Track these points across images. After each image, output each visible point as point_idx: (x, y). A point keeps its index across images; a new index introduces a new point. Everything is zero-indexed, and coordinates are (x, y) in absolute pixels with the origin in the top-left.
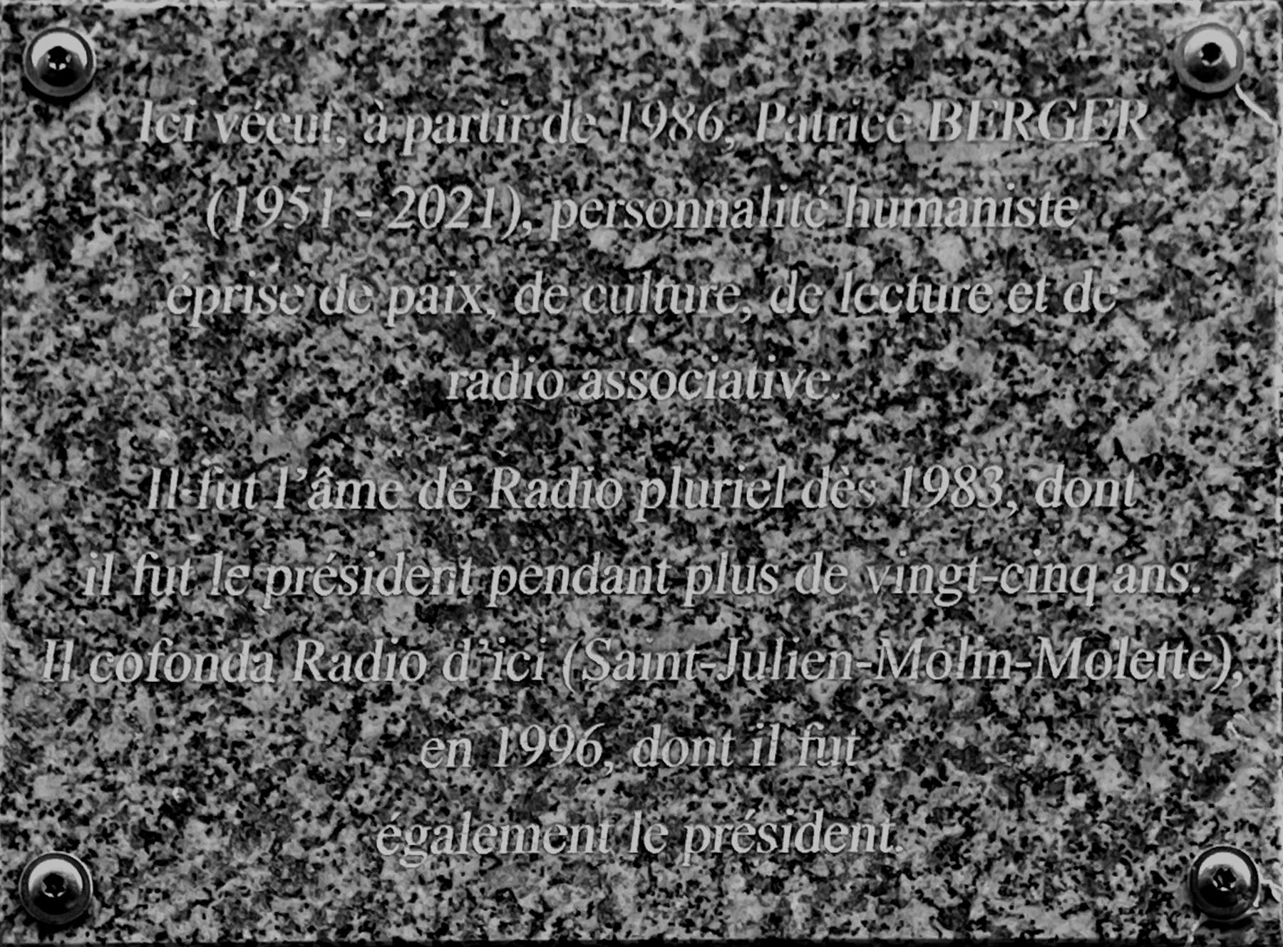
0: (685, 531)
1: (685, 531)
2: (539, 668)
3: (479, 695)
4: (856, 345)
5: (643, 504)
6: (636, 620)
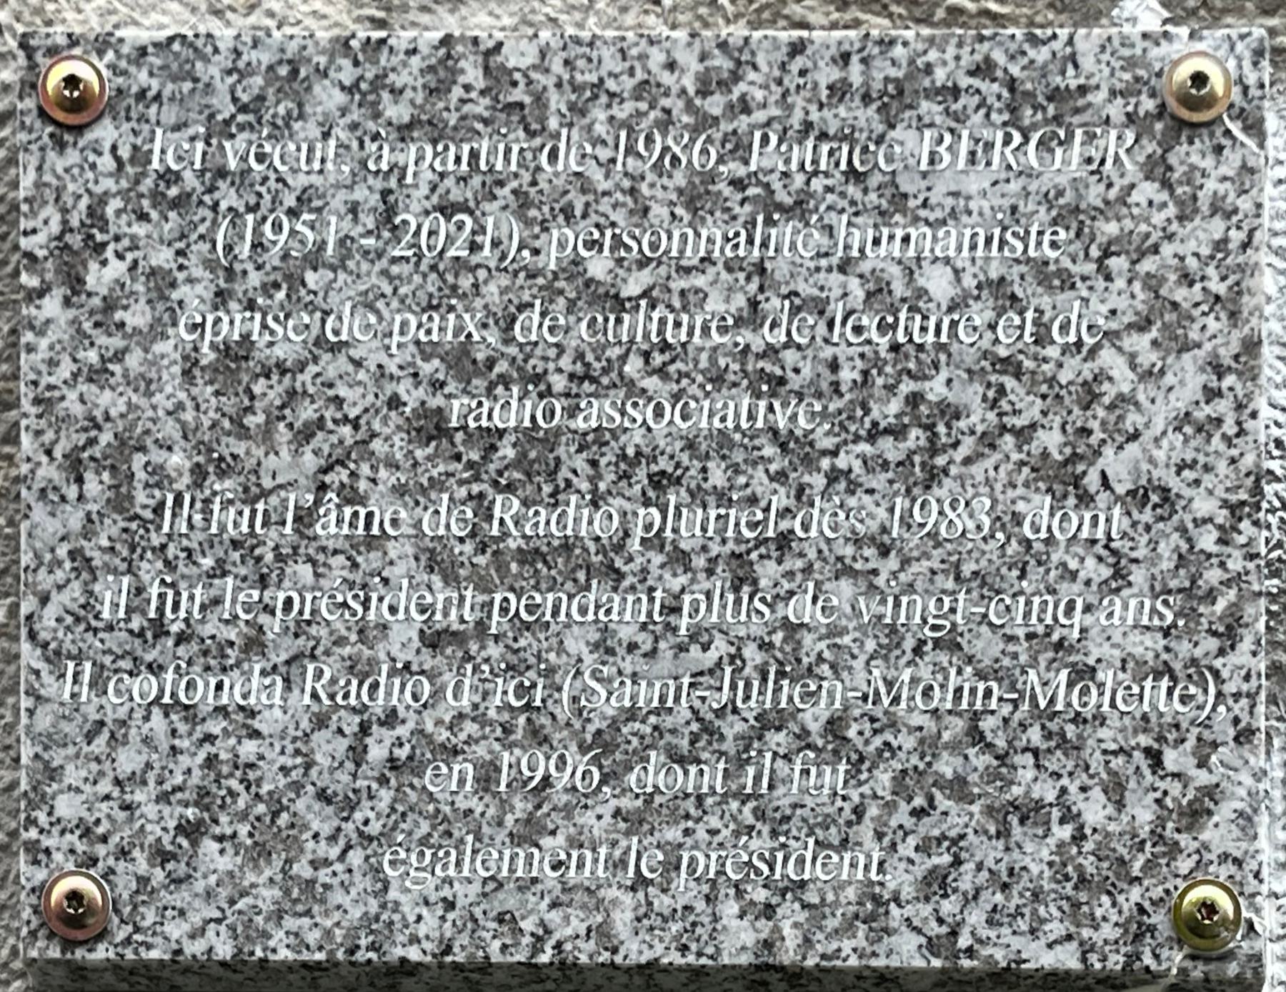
0: (680, 559)
1: (680, 559)
3: (481, 720)
4: (847, 375)
6: (632, 647)
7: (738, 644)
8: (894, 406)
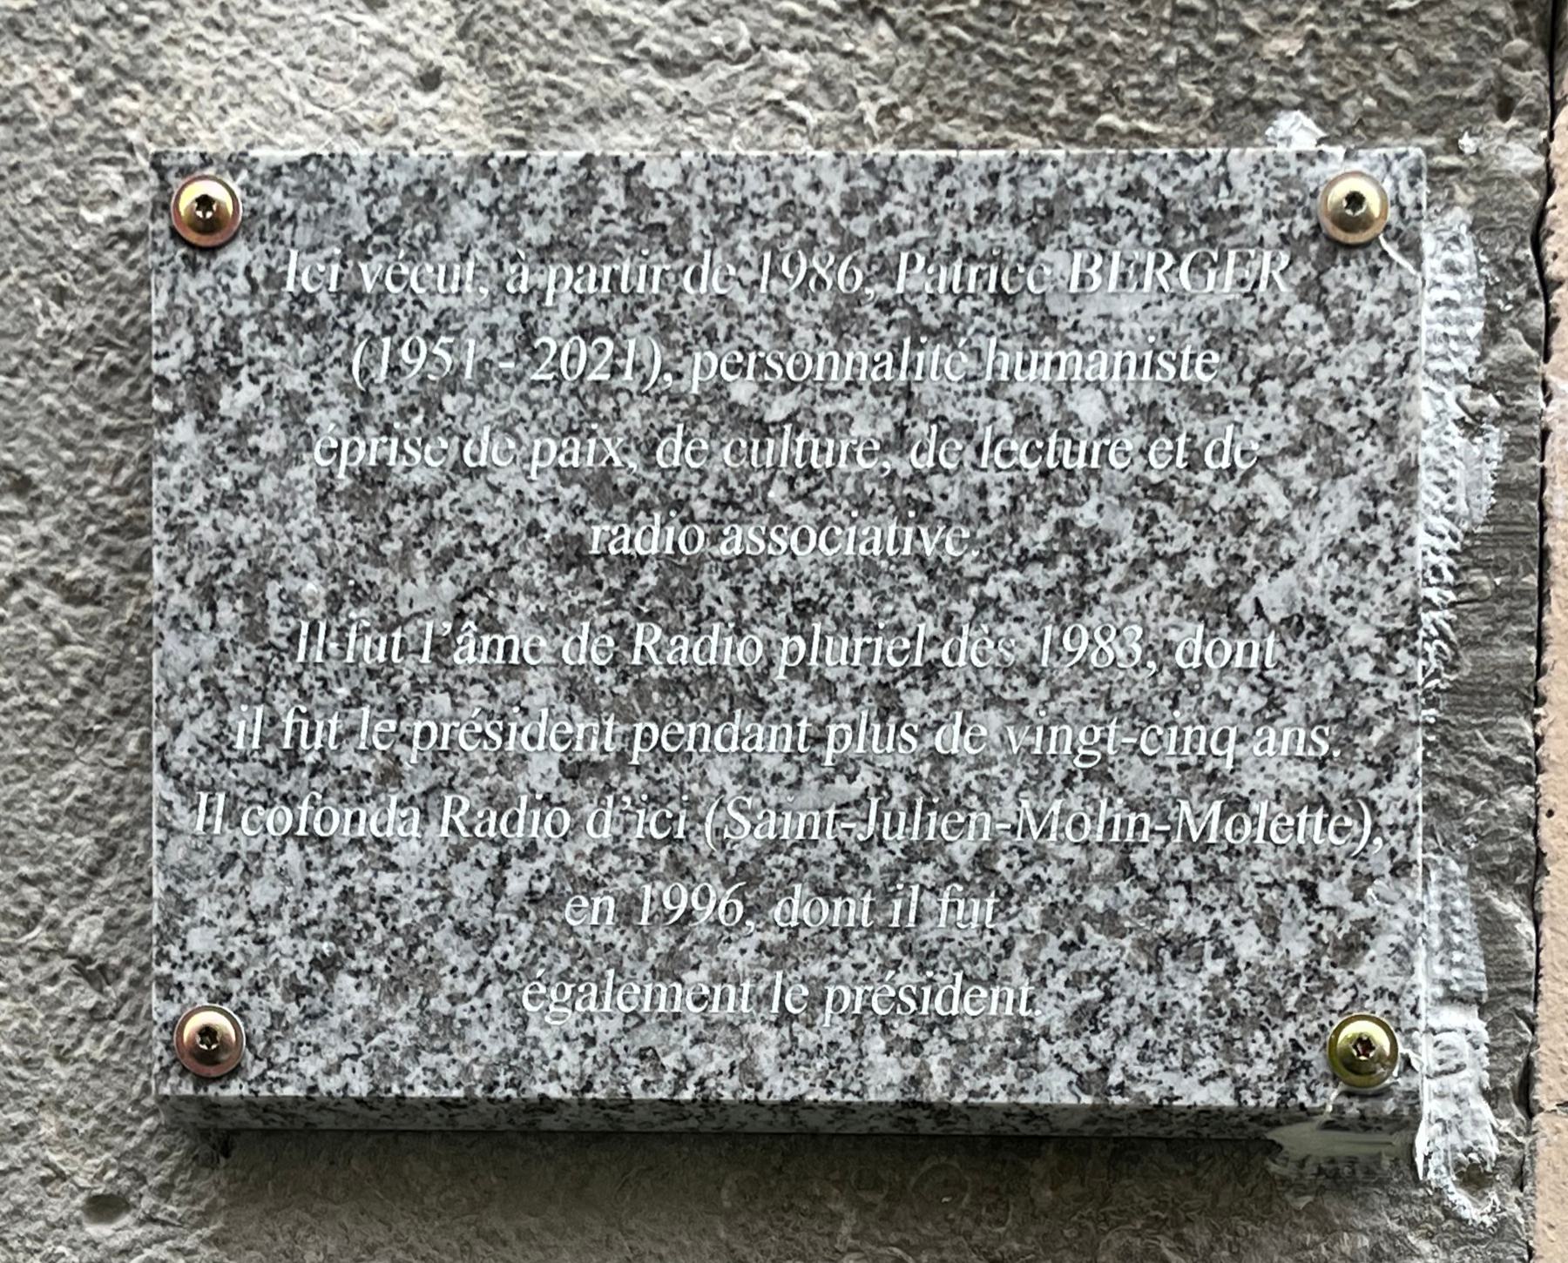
2: (681, 826)
3: (623, 852)
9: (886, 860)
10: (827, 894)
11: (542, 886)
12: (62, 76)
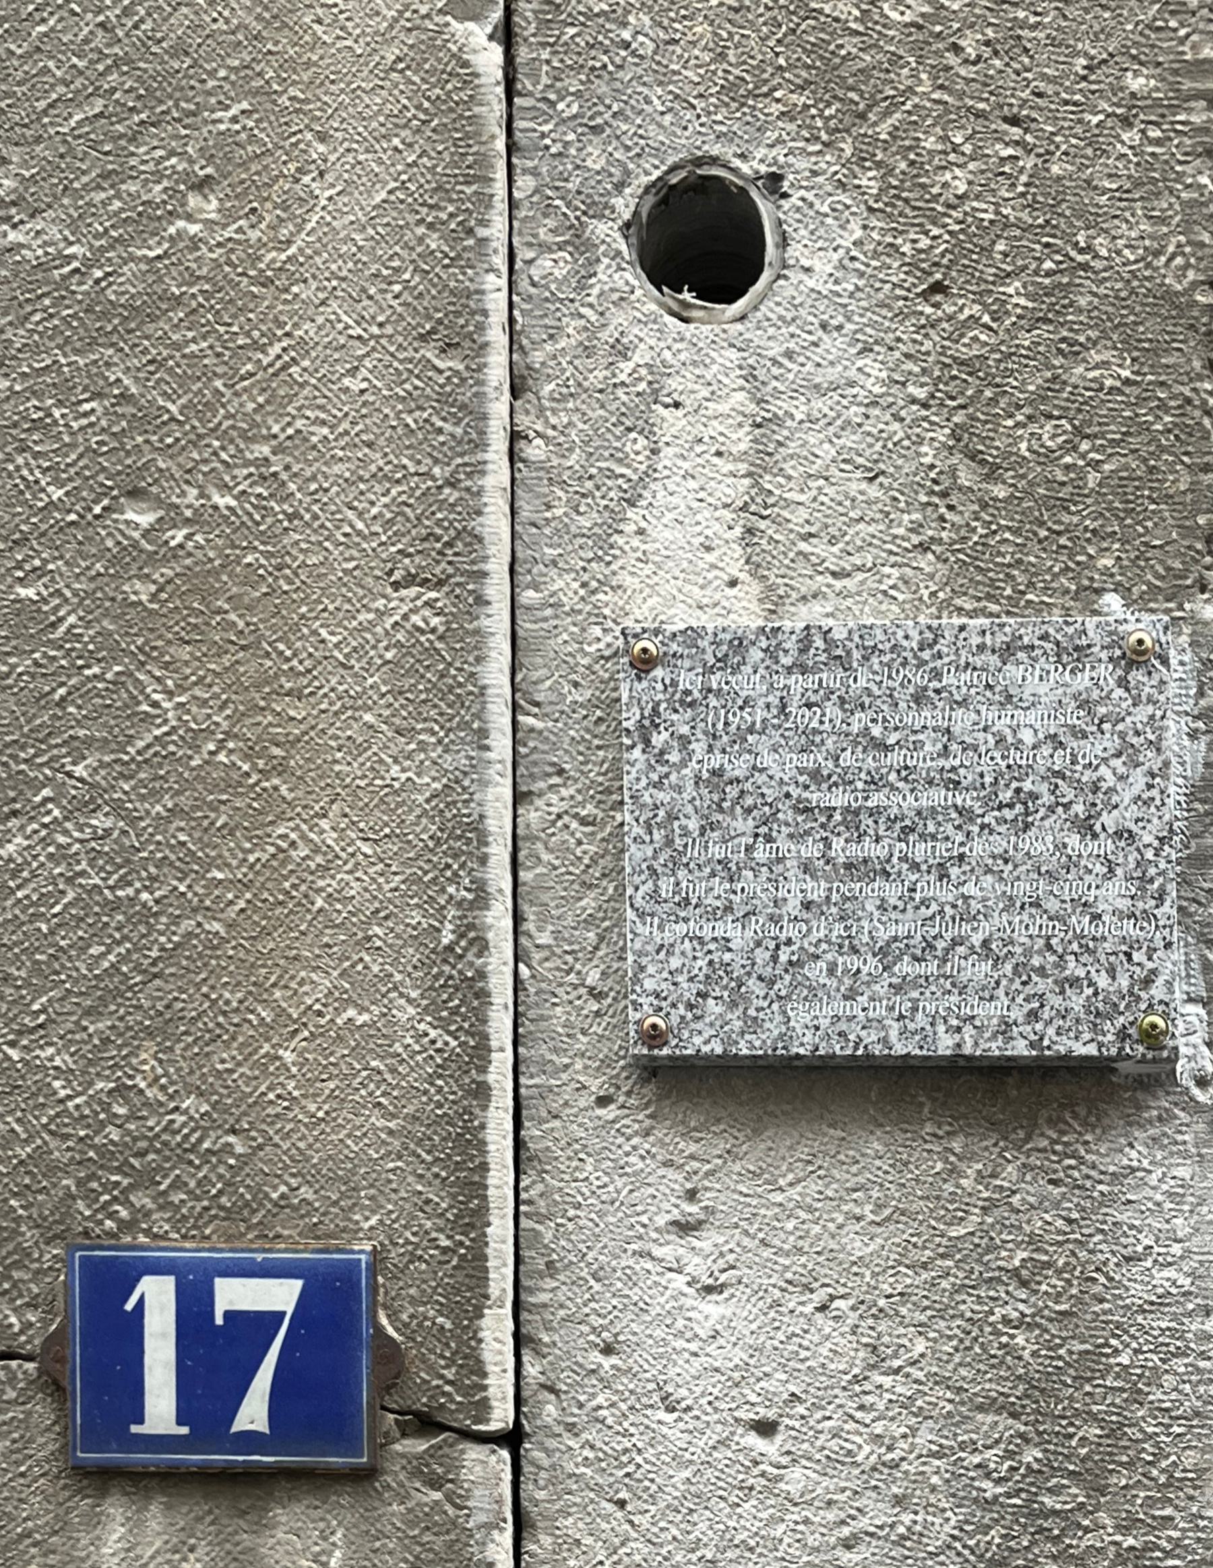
2: (854, 929)
5: (897, 854)
7: (942, 905)
8: (1009, 794)
9: (944, 944)
10: (918, 960)
11: (794, 958)
12: (576, 585)
